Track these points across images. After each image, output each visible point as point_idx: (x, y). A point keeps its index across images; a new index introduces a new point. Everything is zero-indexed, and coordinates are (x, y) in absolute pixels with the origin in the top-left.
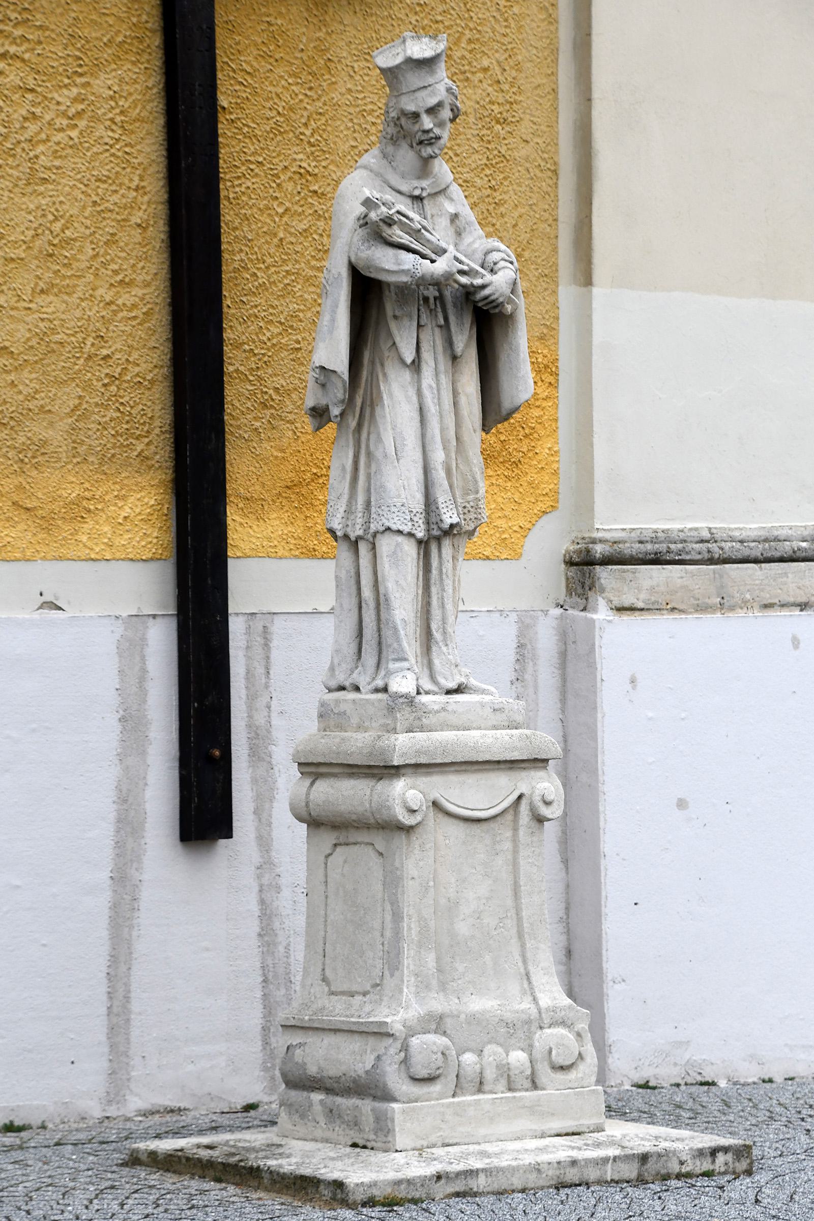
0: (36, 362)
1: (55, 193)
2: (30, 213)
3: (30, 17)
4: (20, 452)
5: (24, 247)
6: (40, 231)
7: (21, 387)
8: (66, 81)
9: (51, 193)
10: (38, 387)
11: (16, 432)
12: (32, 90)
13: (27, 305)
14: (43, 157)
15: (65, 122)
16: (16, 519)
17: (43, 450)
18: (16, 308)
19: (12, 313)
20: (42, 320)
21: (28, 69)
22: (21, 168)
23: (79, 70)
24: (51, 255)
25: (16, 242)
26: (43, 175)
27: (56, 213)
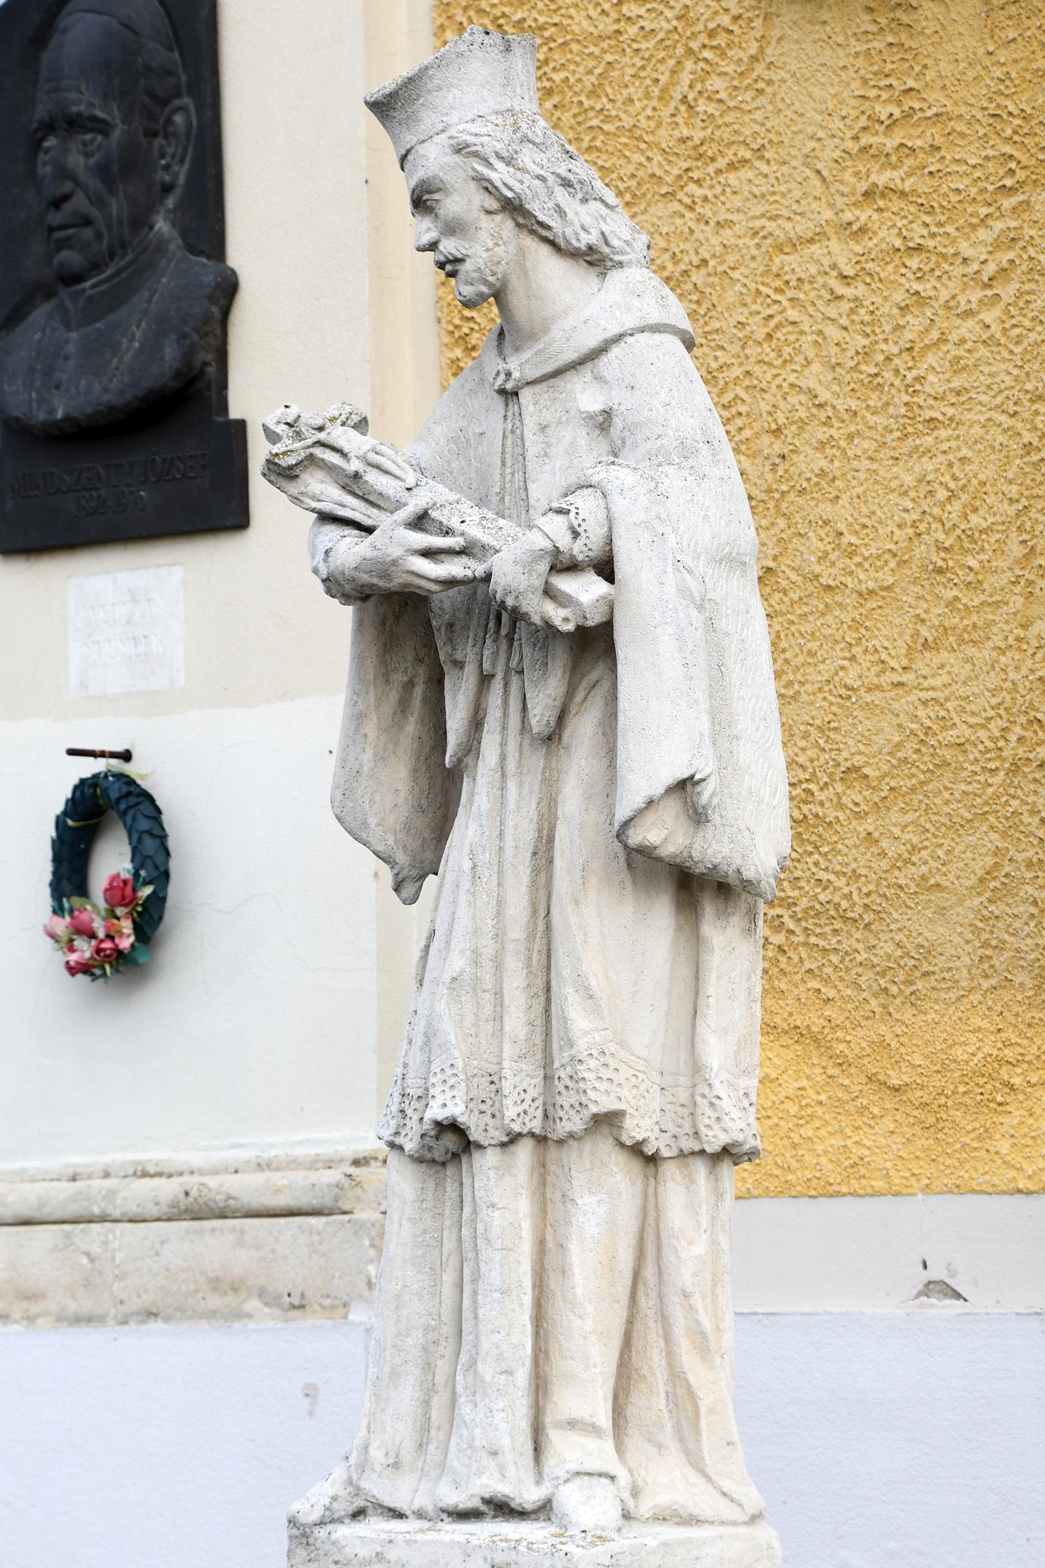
0: (913, 790)
1: (953, 444)
2: (906, 493)
3: (917, 106)
4: (883, 974)
5: (893, 564)
6: (922, 527)
7: (884, 844)
8: (984, 211)
9: (945, 447)
10: (915, 840)
11: (876, 935)
12: (919, 248)
13: (896, 678)
14: (932, 378)
15: (976, 295)
16: (876, 1110)
17: (925, 967)
18: (878, 687)
19: (868, 698)
20: (925, 703)
21: (913, 209)
22: (891, 410)
23: (1008, 182)
24: (940, 571)
25: (878, 557)
26: (928, 414)
27: (952, 485)
